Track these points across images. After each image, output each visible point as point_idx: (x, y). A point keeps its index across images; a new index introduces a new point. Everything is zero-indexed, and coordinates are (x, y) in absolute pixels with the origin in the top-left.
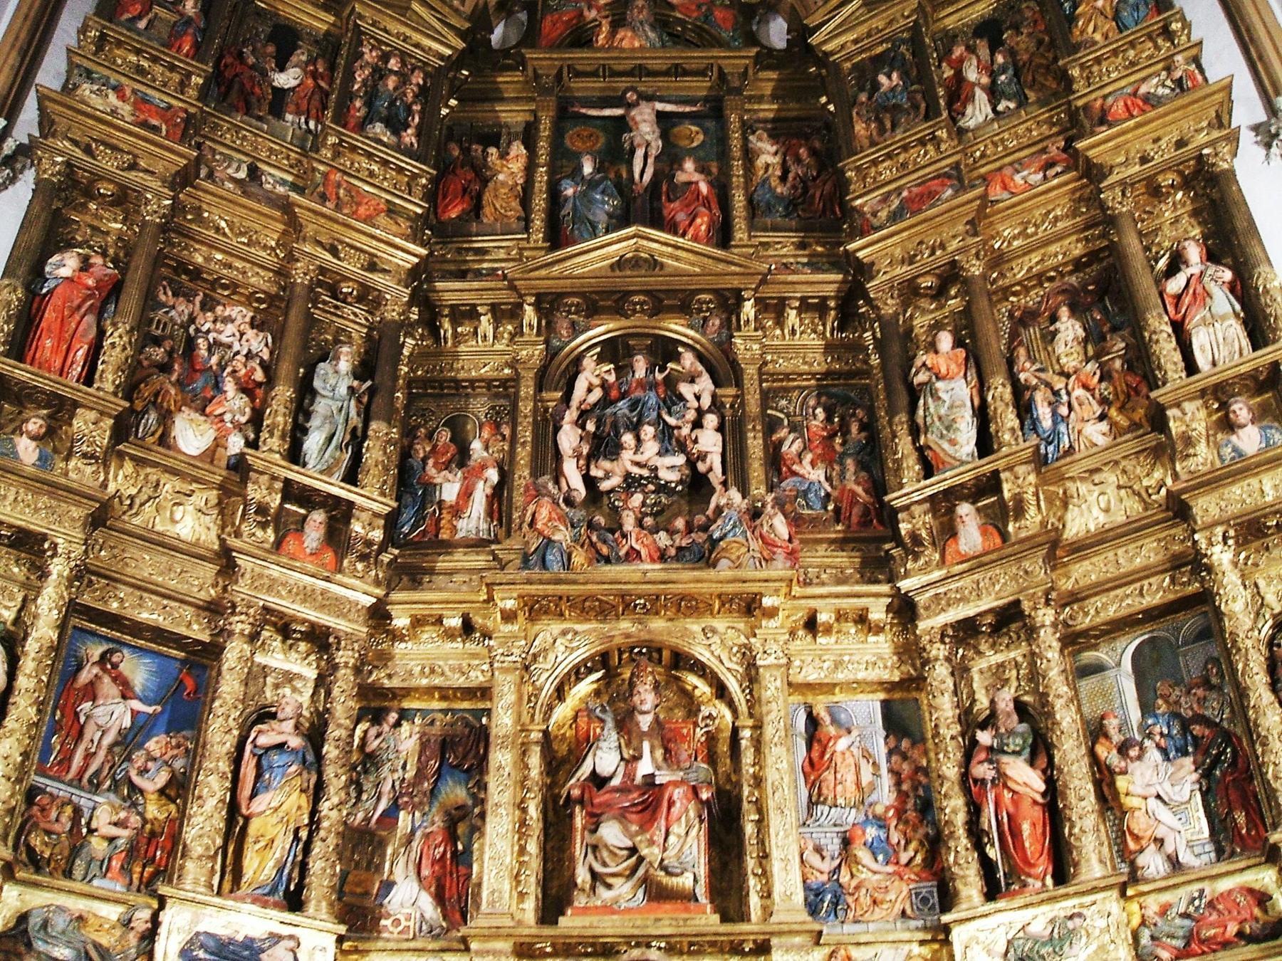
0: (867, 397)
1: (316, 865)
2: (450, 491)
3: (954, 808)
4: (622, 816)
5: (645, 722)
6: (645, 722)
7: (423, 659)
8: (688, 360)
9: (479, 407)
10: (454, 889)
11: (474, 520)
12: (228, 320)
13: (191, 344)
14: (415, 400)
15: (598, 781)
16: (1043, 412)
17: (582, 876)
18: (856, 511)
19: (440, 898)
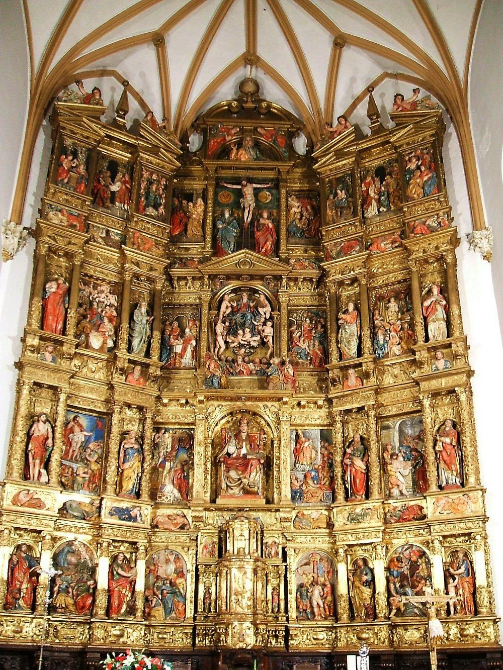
0: (324, 320)
1: (143, 484)
2: (178, 349)
3: (338, 471)
4: (236, 469)
5: (244, 436)
6: (244, 436)
7: (172, 412)
8: (262, 298)
9: (188, 313)
10: (184, 487)
11: (187, 360)
12: (102, 292)
13: (91, 303)
14: (164, 312)
15: (228, 454)
16: (381, 338)
17: (224, 486)
18: (318, 361)
19: (180, 491)
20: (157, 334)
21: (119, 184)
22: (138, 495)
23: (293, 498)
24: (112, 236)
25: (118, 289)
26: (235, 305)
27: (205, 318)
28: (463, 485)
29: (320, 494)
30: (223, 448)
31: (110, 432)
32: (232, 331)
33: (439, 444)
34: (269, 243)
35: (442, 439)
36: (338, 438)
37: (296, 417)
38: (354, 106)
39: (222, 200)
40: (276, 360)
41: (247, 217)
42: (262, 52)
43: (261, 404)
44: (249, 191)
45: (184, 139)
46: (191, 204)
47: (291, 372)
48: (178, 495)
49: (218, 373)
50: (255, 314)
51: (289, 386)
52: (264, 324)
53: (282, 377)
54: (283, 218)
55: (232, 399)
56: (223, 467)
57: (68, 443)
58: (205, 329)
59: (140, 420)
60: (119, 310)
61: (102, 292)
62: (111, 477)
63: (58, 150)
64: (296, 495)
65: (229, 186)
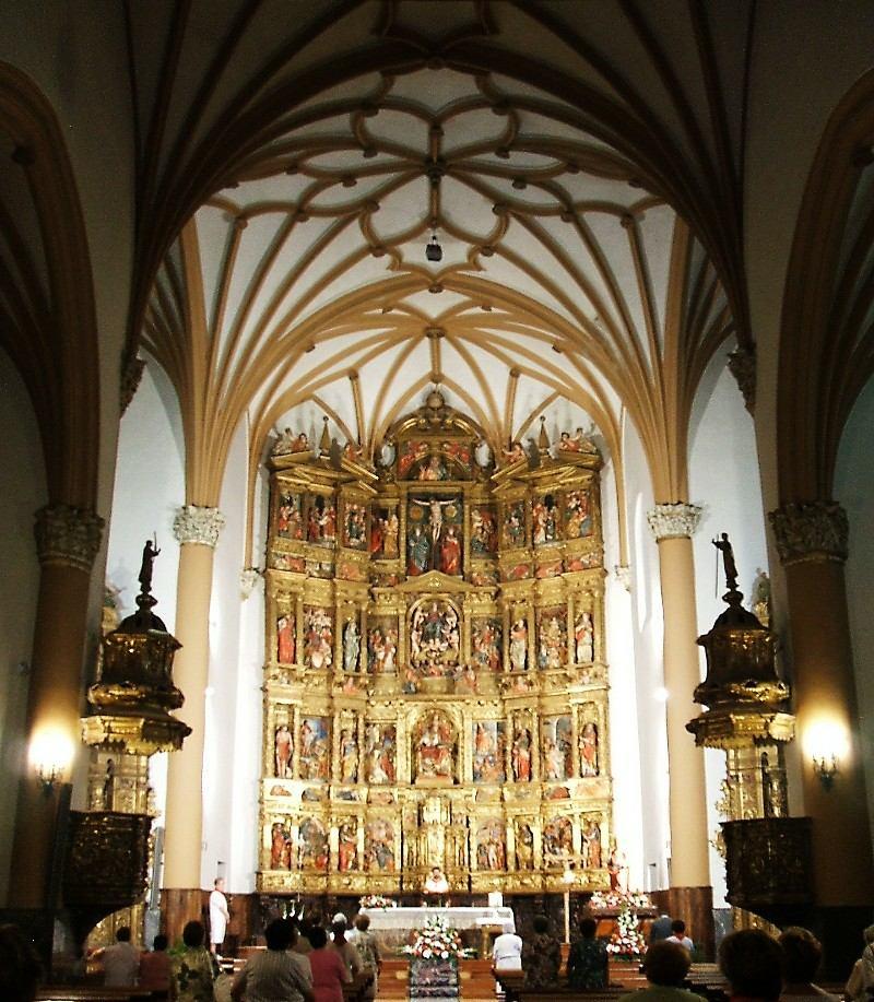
0: (500, 628)
1: (359, 771)
2: (381, 656)
3: (509, 759)
4: (430, 756)
5: (436, 729)
6: (436, 729)
7: (379, 712)
8: (449, 608)
9: (388, 623)
10: (390, 770)
11: (389, 664)
12: (318, 616)
13: (311, 627)
14: (370, 627)
15: (424, 744)
16: (544, 652)
17: (421, 770)
18: (495, 663)
19: (387, 772)
20: (364, 649)
21: (326, 518)
22: (356, 780)
23: (474, 778)
24: (324, 567)
25: (331, 612)
26: (427, 615)
27: (402, 630)
28: (598, 773)
29: (496, 774)
30: (419, 739)
31: (332, 732)
32: (425, 638)
33: (581, 743)
34: (454, 561)
35: (585, 740)
36: (510, 731)
37: (476, 715)
38: (531, 419)
39: (414, 516)
40: (460, 668)
41: (436, 535)
42: (445, 370)
43: (448, 704)
44: (436, 509)
45: (378, 455)
46: (386, 522)
47: (473, 678)
48: (385, 776)
49: (415, 679)
50: (444, 623)
51: (471, 690)
52: (451, 631)
53: (465, 682)
54: (467, 529)
55: (426, 701)
56: (420, 754)
57: (302, 743)
58: (402, 639)
59: (328, 676)
60: (333, 630)
61: (318, 616)
62: (336, 768)
63: (275, 500)
64: (477, 776)
65: (419, 502)
